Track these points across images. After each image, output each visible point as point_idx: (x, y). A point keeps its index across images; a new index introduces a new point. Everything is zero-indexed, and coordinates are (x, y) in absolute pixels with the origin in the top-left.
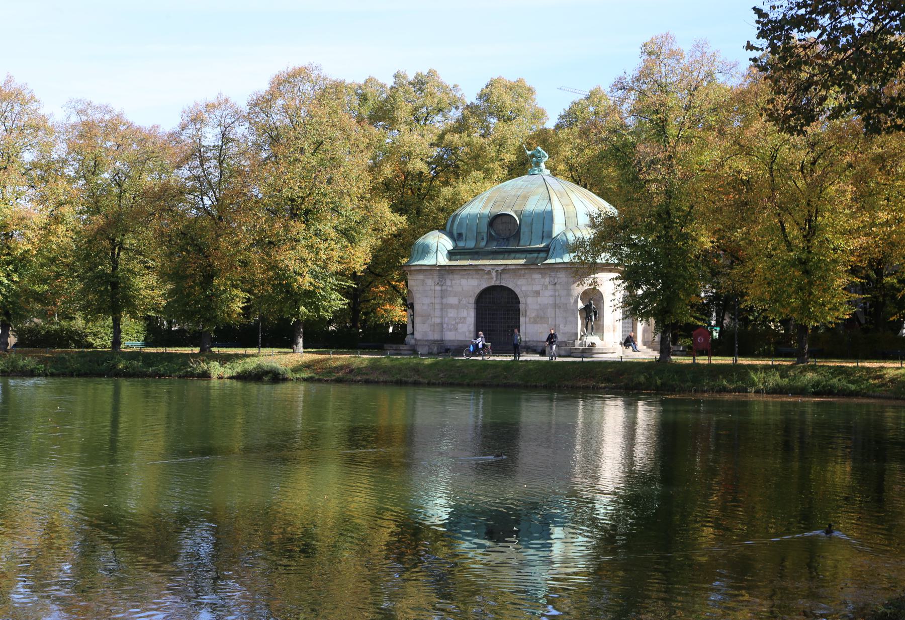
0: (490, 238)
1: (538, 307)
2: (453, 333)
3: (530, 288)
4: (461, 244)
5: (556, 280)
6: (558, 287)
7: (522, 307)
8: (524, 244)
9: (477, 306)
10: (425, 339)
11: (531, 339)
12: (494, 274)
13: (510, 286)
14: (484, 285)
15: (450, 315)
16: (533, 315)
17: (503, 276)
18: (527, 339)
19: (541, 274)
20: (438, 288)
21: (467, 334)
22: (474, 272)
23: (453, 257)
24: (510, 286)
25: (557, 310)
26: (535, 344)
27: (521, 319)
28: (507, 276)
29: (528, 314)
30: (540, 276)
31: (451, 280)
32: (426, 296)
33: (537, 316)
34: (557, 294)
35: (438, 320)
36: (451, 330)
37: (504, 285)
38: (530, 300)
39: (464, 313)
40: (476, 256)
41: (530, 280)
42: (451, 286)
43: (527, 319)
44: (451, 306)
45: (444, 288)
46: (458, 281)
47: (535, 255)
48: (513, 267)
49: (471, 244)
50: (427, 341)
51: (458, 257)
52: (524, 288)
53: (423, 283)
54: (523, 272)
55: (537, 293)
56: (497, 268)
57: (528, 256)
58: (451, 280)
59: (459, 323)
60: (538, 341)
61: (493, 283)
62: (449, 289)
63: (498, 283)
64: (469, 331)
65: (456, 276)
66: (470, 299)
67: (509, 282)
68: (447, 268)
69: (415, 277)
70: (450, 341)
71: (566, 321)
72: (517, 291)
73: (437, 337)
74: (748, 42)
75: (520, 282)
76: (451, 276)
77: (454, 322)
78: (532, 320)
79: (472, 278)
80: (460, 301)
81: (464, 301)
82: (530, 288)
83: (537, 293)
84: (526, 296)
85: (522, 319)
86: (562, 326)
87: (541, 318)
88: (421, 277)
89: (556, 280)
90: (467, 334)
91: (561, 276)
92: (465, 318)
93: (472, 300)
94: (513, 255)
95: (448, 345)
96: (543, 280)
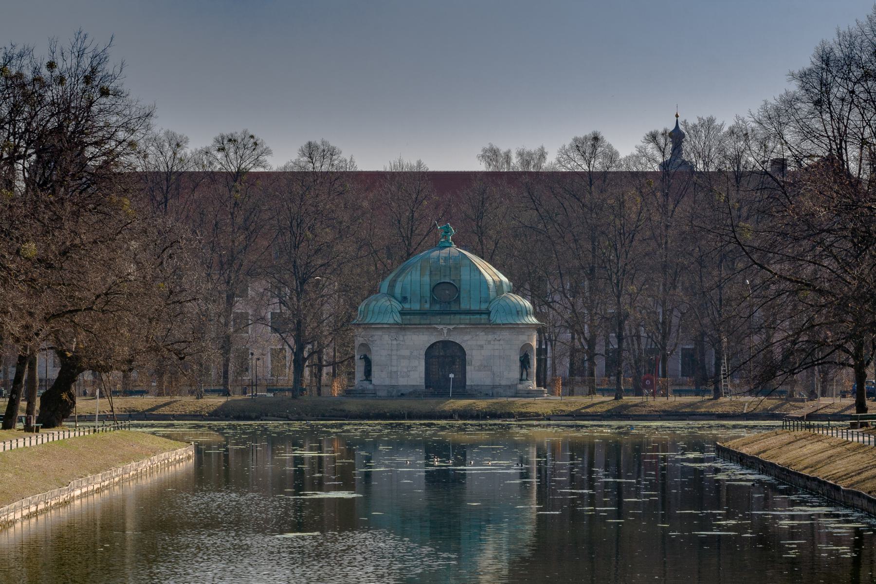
0: (433, 301)
4: (407, 306)
5: (501, 337)
6: (502, 342)
7: (467, 357)
8: (464, 306)
10: (383, 384)
12: (445, 331)
14: (434, 340)
20: (395, 342)
24: (457, 341)
25: (501, 361)
27: (467, 367)
29: (473, 363)
31: (403, 336)
35: (394, 369)
36: (403, 377)
37: (452, 340)
38: (474, 352)
39: (415, 363)
43: (473, 368)
44: (404, 357)
45: (398, 342)
47: (478, 316)
49: (416, 306)
50: (385, 386)
54: (468, 330)
55: (482, 347)
57: (472, 317)
58: (403, 336)
61: (441, 338)
62: (401, 343)
63: (447, 338)
65: (408, 333)
67: (457, 339)
72: (463, 345)
73: (394, 383)
74: (685, 121)
75: (466, 337)
77: (405, 370)
79: (423, 335)
80: (411, 353)
85: (468, 368)
87: (485, 366)
88: (379, 333)
89: (501, 337)
92: (416, 367)
93: (423, 352)
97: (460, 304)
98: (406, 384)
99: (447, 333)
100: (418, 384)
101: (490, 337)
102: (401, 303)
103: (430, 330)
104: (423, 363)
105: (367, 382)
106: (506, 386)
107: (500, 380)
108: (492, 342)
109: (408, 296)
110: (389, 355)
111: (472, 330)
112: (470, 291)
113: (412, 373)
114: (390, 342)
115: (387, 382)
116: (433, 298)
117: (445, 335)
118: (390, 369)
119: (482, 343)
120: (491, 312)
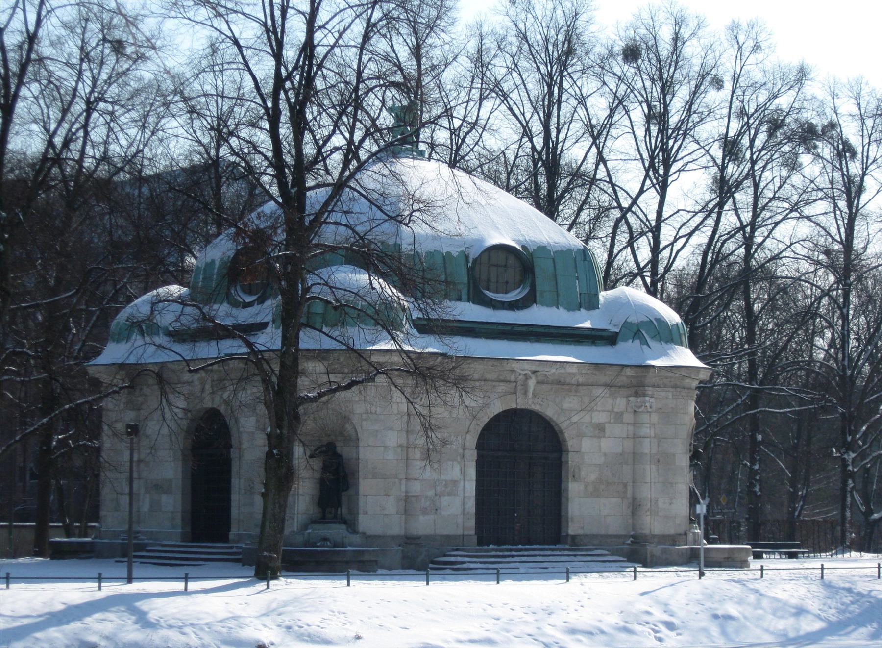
1: (600, 460)
2: (431, 517)
9: (479, 456)
13: (549, 412)
14: (497, 407)
16: (593, 477)
38: (587, 444)
43: (582, 487)
55: (600, 430)
78: (590, 488)
84: (581, 435)
92: (455, 482)
93: (472, 441)
98: (432, 533)
113: (445, 500)
115: (396, 528)
118: (403, 488)
119: (600, 417)
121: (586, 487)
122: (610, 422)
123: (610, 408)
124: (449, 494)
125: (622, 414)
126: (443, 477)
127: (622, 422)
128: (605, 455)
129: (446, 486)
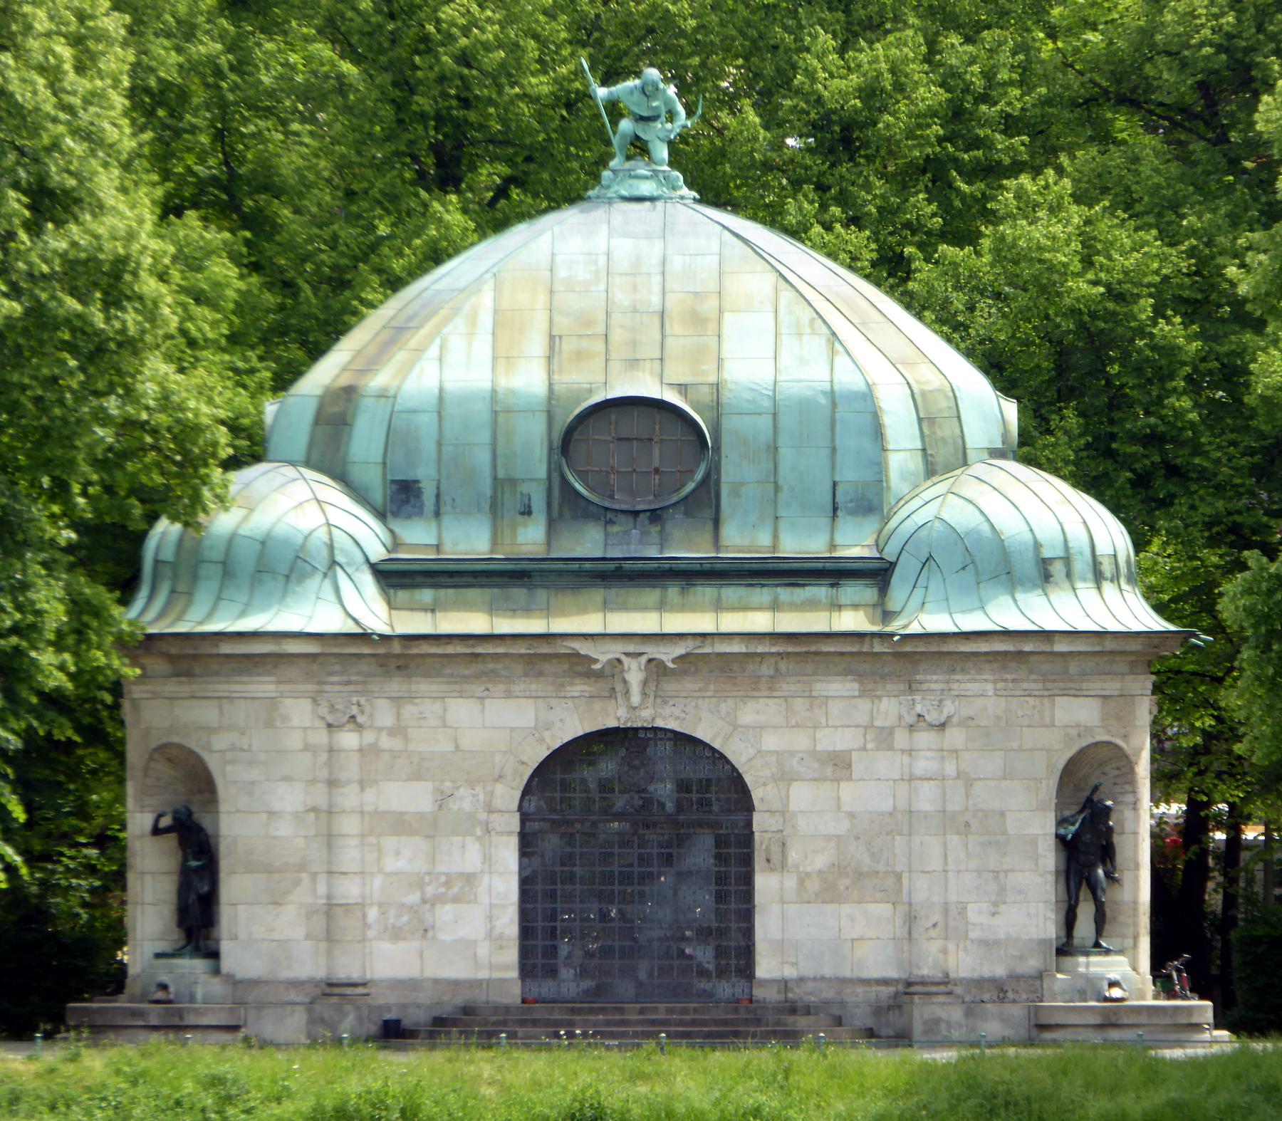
3: (801, 741)
6: (955, 736)
7: (761, 822)
11: (808, 971)
12: (634, 674)
15: (391, 864)
16: (820, 862)
17: (669, 687)
18: (790, 972)
19: (860, 677)
21: (483, 951)
22: (518, 668)
23: (402, 595)
25: (954, 840)
26: (829, 994)
28: (690, 685)
29: (793, 856)
30: (851, 687)
32: (288, 779)
33: (839, 869)
34: (950, 769)
36: (396, 934)
39: (467, 856)
40: (519, 593)
41: (800, 704)
42: (398, 730)
43: (791, 882)
46: (431, 708)
48: (737, 647)
50: (294, 984)
51: (426, 595)
52: (771, 742)
53: (271, 717)
54: (766, 669)
55: (840, 764)
56: (653, 651)
59: (439, 899)
60: (844, 981)
62: (386, 742)
63: (644, 717)
64: (494, 938)
65: (424, 686)
66: (499, 788)
68: (396, 648)
69: (222, 688)
70: (397, 984)
71: (1002, 890)
72: (739, 753)
76: (396, 686)
78: (813, 885)
80: (443, 799)
81: (465, 800)
82: (801, 741)
83: (840, 764)
84: (786, 778)
85: (765, 883)
86: (977, 913)
88: (264, 686)
89: (949, 708)
90: (483, 951)
91: (974, 687)
93: (508, 796)
94: (705, 592)
95: (390, 1004)
96: (865, 705)
97: (716, 522)
99: (645, 682)
100: (483, 974)
101: (889, 708)
102: (381, 515)
103: (547, 667)
104: (508, 855)
105: (195, 966)
106: (980, 983)
107: (945, 951)
108: (901, 738)
109: (425, 473)
110: (314, 810)
111: (783, 666)
112: (774, 449)
113: (445, 913)
114: (320, 737)
116: (565, 482)
117: (636, 698)
119: (842, 740)
120: (892, 565)
121: (801, 882)
122: (864, 749)
123: (864, 720)
124: (456, 900)
125: (890, 731)
126: (441, 868)
127: (891, 748)
128: (852, 815)
129: (448, 884)
